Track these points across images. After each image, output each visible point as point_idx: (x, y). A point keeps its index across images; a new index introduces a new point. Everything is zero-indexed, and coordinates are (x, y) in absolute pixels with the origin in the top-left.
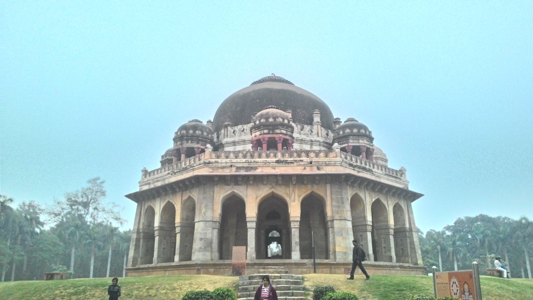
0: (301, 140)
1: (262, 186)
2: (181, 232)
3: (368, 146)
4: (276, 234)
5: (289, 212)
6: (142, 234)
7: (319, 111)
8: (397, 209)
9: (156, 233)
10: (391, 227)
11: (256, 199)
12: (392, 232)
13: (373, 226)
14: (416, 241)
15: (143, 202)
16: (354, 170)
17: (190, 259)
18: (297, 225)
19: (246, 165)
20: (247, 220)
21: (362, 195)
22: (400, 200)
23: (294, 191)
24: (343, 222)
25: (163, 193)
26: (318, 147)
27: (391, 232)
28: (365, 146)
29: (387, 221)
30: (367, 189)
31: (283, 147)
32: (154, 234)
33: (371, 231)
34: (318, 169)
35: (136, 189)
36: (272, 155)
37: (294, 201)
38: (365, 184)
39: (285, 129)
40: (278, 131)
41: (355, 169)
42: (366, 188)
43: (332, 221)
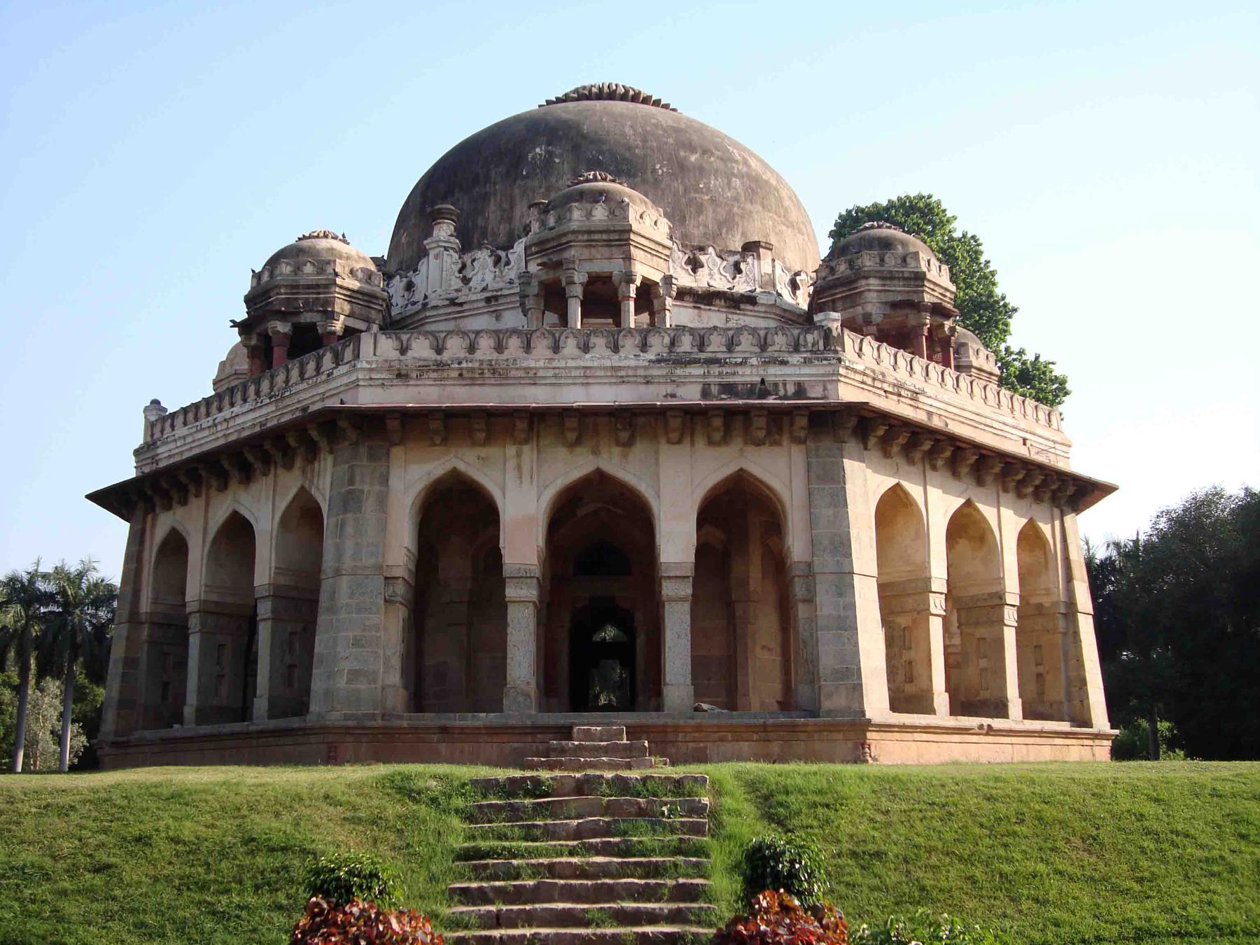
1: (562, 452)
2: (276, 618)
5: (658, 544)
6: (145, 632)
8: (1030, 539)
9: (194, 623)
10: (1008, 602)
11: (539, 497)
12: (1010, 616)
13: (949, 596)
15: (150, 518)
17: (302, 708)
18: (687, 589)
20: (507, 571)
21: (914, 490)
25: (214, 483)
27: (1006, 616)
29: (1001, 580)
30: (934, 468)
31: (637, 312)
32: (186, 628)
33: (944, 613)
35: (126, 470)
36: (599, 342)
38: (927, 446)
42: (928, 467)
43: (810, 573)
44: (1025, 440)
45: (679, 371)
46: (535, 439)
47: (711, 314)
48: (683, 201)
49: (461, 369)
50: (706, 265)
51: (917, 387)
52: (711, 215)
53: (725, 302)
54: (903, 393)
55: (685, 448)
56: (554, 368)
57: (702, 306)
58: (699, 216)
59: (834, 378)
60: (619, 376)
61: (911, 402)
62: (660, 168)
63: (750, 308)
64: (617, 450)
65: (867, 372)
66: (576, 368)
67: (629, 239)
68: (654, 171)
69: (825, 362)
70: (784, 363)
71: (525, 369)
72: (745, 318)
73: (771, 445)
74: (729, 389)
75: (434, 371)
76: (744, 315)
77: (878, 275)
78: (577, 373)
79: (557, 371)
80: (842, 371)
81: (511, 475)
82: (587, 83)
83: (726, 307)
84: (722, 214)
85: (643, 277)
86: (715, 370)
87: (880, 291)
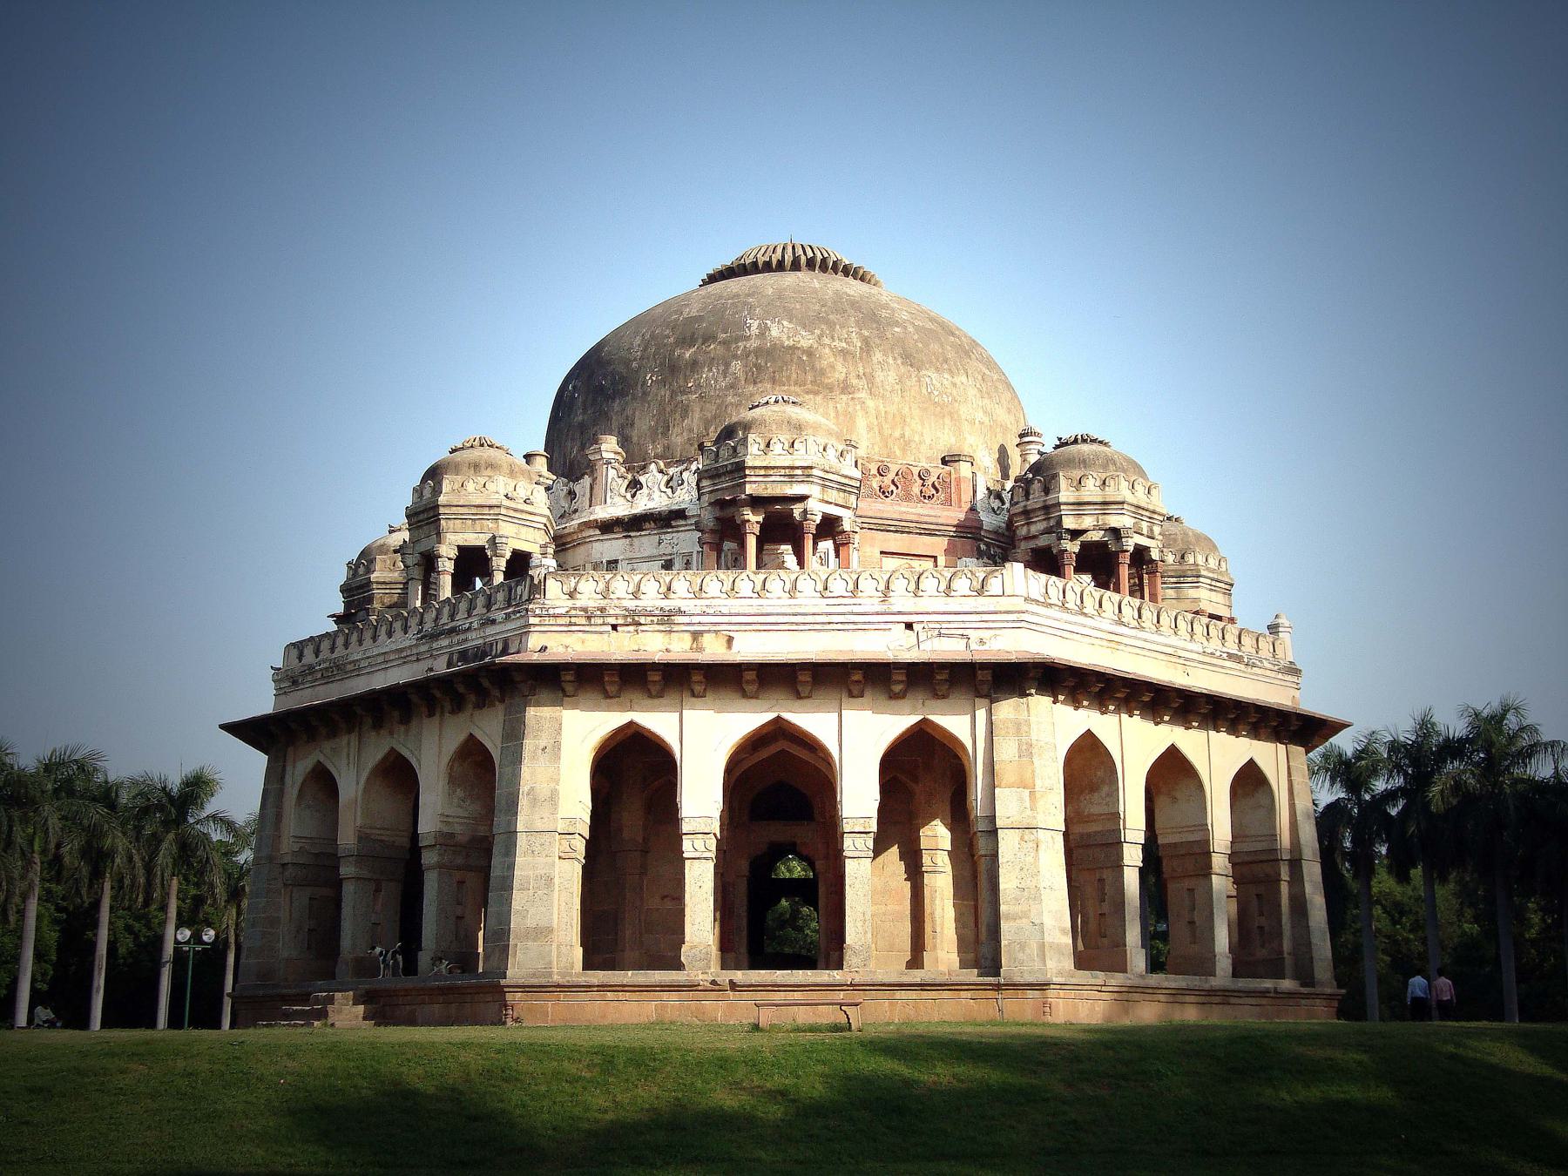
4: (794, 869)
44: (909, 626)
45: (435, 645)
46: (357, 729)
47: (644, 540)
48: (668, 409)
49: (321, 670)
50: (645, 486)
51: (667, 609)
52: (697, 415)
53: (656, 524)
54: (642, 621)
55: (436, 719)
56: (368, 658)
57: (632, 534)
58: (683, 421)
59: (525, 631)
60: (404, 657)
61: (662, 628)
62: (651, 378)
63: (683, 522)
64: (402, 728)
65: (573, 612)
66: (378, 655)
67: (440, 514)
68: (645, 382)
69: (518, 615)
70: (493, 622)
71: (353, 661)
72: (682, 534)
73: (479, 706)
74: (464, 656)
75: (310, 674)
76: (678, 532)
77: (706, 475)
78: (380, 659)
79: (369, 660)
80: (532, 620)
81: (344, 761)
82: (780, 239)
83: (658, 528)
84: (711, 409)
85: (458, 546)
86: (455, 640)
87: (711, 492)
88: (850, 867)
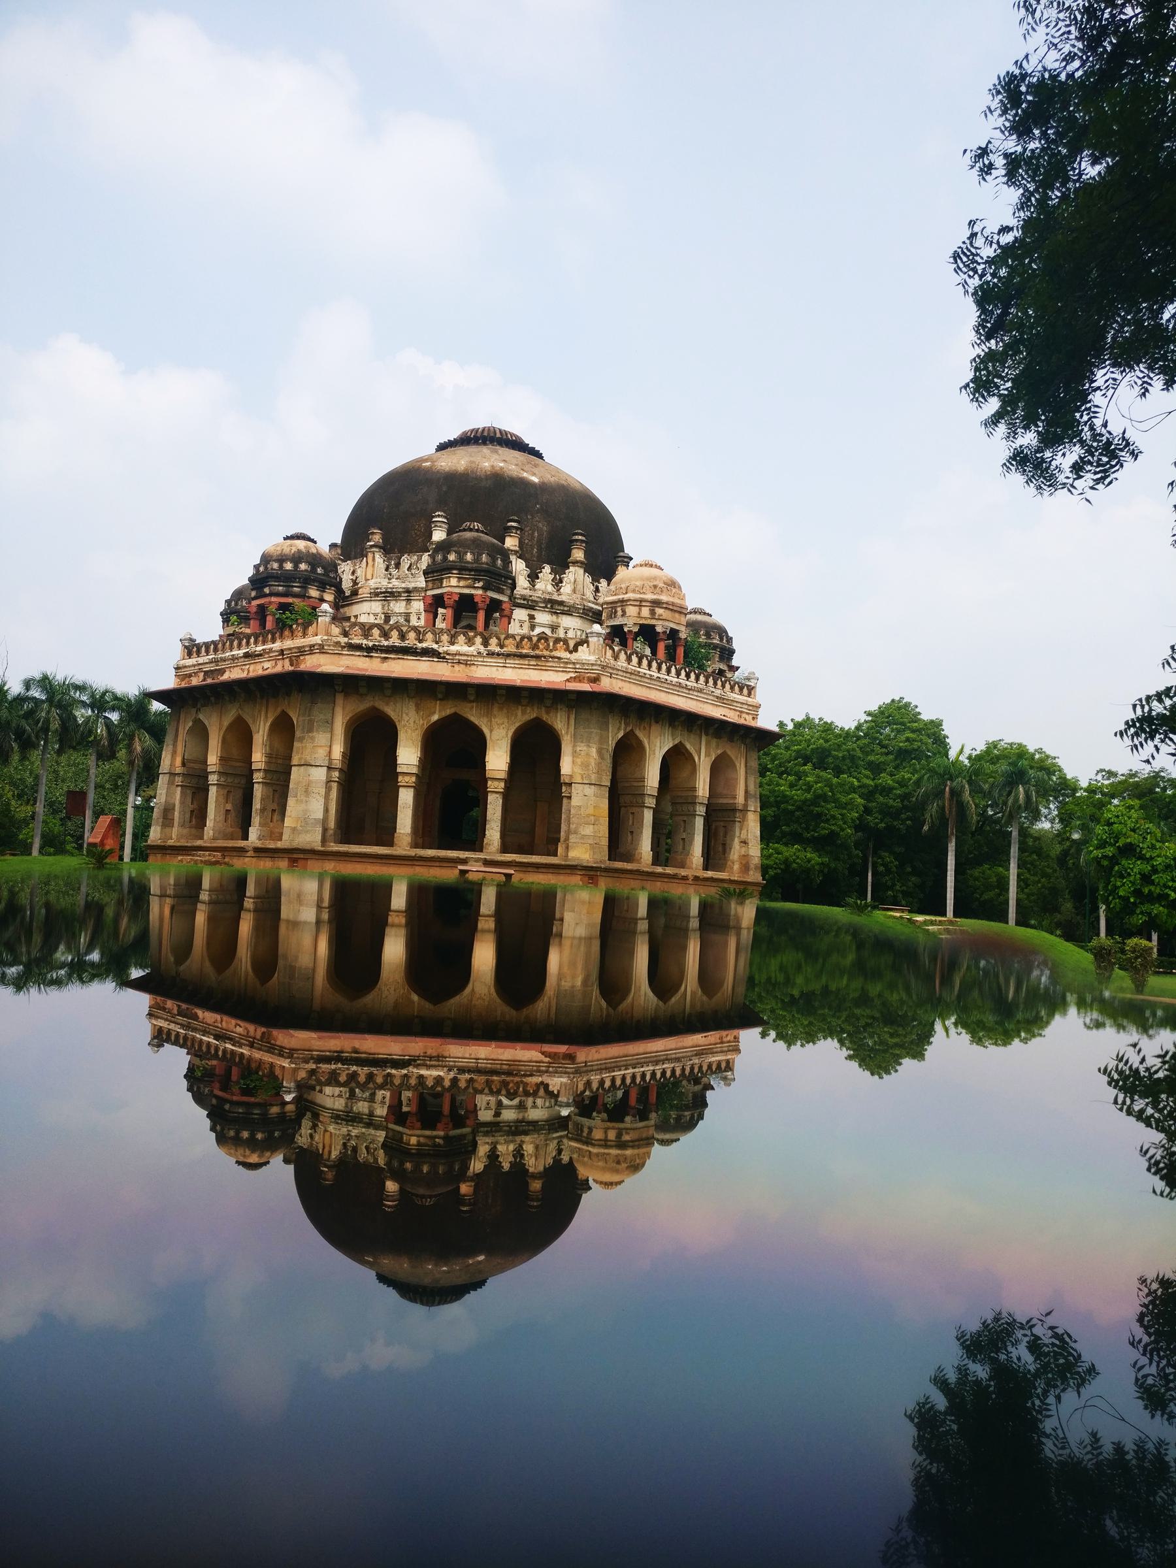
0: (381, 593)
3: (466, 591)
7: (445, 517)
14: (580, 807)
16: (366, 656)
19: (212, 667)
22: (548, 713)
23: (260, 711)
24: (303, 767)
26: (404, 603)
28: (451, 594)
34: (292, 665)
37: (258, 732)
39: (282, 584)
40: (267, 590)
41: (372, 654)
88: (491, 798)
